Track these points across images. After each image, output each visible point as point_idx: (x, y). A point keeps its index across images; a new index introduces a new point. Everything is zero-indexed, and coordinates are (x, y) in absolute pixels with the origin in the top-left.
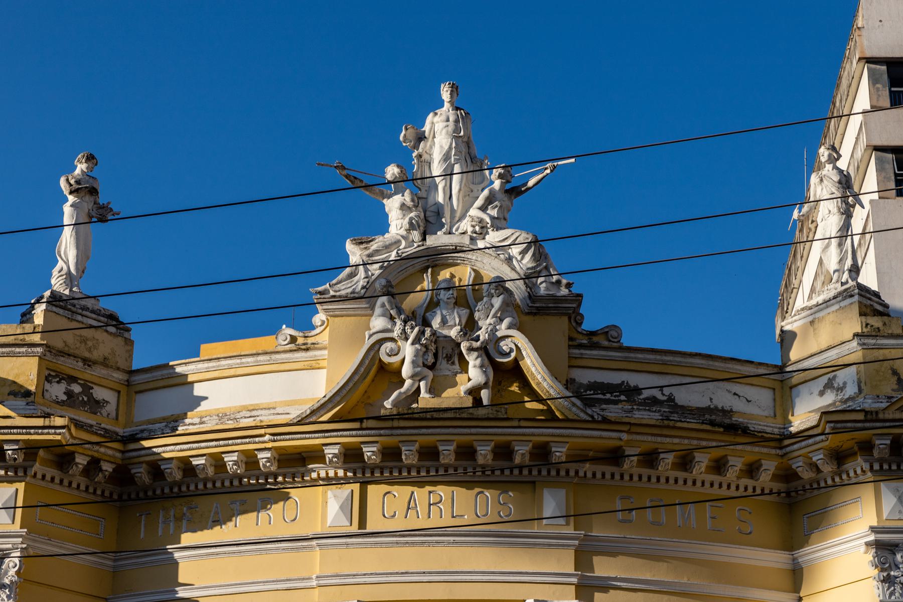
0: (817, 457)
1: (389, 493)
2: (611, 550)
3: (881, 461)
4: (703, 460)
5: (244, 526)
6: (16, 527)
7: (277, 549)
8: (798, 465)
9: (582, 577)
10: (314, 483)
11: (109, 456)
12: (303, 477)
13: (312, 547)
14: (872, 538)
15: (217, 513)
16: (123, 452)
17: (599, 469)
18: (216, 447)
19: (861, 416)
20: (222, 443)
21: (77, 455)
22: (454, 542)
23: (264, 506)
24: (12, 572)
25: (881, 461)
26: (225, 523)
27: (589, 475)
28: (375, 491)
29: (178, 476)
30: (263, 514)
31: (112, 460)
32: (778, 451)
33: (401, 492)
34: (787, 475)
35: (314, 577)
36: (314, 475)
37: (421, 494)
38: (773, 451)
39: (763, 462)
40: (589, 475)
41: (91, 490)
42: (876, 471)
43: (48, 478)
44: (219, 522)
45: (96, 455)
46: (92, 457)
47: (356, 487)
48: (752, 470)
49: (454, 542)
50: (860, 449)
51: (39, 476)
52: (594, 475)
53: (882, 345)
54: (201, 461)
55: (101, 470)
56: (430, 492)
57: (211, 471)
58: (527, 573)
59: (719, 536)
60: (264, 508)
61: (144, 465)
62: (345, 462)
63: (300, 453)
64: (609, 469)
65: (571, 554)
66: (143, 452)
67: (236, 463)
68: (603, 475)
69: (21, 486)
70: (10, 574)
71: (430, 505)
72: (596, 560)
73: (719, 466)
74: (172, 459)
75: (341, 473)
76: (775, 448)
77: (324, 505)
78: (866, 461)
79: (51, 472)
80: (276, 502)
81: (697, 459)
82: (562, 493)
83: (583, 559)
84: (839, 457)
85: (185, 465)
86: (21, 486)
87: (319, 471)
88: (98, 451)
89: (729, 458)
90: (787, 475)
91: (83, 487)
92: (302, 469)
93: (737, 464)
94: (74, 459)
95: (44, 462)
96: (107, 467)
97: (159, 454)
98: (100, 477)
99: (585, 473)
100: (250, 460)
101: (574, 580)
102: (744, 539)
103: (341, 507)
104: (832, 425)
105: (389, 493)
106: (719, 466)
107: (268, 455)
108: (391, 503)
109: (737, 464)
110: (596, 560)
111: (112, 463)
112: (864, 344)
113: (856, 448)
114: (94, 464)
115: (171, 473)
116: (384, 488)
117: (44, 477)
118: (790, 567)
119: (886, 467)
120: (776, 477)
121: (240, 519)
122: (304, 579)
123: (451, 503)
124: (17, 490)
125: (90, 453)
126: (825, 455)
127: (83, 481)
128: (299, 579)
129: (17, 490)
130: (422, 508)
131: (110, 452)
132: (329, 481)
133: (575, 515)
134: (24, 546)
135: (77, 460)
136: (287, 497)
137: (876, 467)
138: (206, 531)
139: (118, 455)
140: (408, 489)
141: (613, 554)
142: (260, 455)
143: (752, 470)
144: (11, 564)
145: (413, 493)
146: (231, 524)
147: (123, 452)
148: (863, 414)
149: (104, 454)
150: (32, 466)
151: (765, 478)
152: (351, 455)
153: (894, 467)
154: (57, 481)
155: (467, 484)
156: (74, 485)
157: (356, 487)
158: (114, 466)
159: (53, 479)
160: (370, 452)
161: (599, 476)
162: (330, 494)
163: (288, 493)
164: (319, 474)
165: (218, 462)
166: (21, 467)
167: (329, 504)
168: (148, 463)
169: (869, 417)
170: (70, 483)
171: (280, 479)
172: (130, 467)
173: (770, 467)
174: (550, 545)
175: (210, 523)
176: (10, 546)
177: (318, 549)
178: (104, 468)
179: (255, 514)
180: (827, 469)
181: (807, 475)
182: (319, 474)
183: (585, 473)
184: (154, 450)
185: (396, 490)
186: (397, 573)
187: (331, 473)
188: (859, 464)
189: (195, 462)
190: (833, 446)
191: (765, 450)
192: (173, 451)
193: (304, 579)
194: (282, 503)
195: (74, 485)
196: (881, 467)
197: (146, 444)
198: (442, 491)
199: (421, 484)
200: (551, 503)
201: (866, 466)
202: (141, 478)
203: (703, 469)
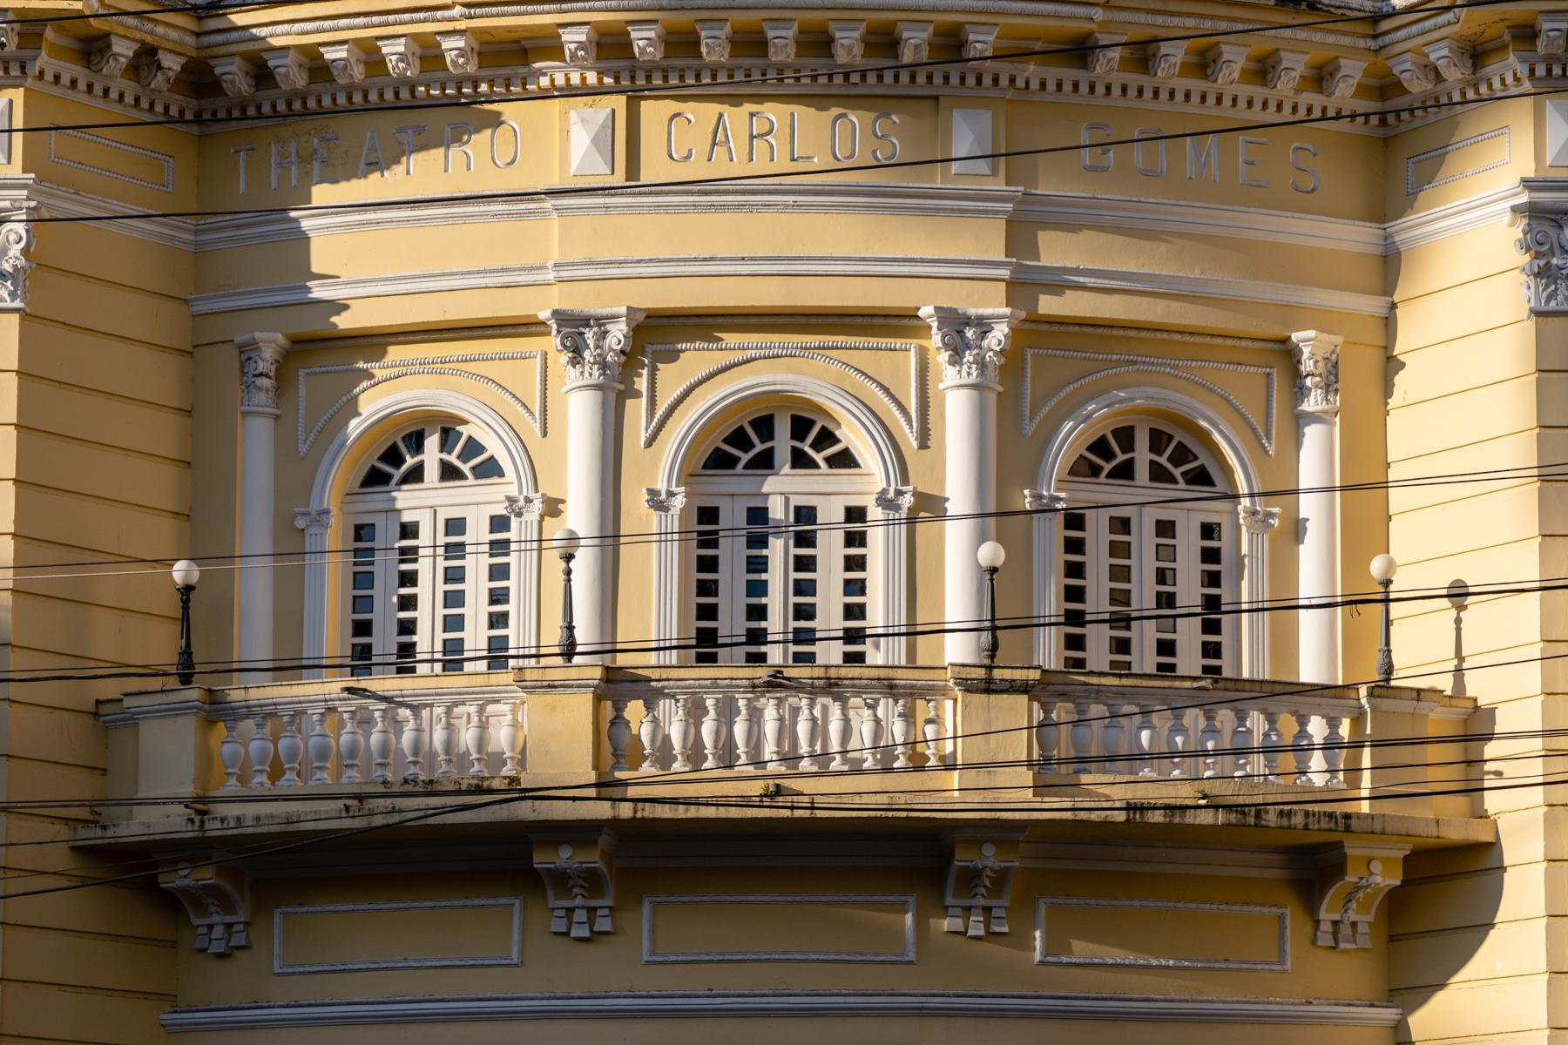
0: (1438, 54)
1: (678, 115)
2: (1069, 220)
3: (1549, 61)
4: (1236, 58)
5: (423, 172)
6: (15, 170)
7: (483, 215)
8: (1404, 69)
9: (1018, 268)
10: (545, 96)
11: (174, 41)
12: (524, 85)
13: (544, 212)
14: (1524, 198)
15: (373, 149)
16: (198, 35)
17: (1053, 73)
18: (365, 27)
20: (375, 19)
21: (114, 40)
22: (796, 205)
23: (456, 136)
24: (15, 250)
25: (1549, 61)
26: (388, 168)
27: (1035, 85)
28: (653, 112)
29: (300, 80)
30: (455, 152)
31: (179, 49)
33: (702, 114)
34: (1385, 87)
35: (550, 264)
36: (545, 82)
37: (736, 117)
40: (1035, 85)
41: (145, 104)
42: (1540, 79)
43: (65, 80)
44: (377, 164)
45: (149, 39)
46: (143, 43)
47: (620, 102)
48: (1321, 77)
49: (796, 205)
50: (1515, 37)
51: (49, 77)
52: (1043, 85)
54: (339, 53)
55: (160, 67)
56: (752, 115)
57: (358, 72)
58: (922, 261)
59: (1258, 196)
60: (457, 139)
61: (237, 59)
62: (599, 58)
63: (517, 41)
64: (1069, 74)
65: (998, 228)
66: (234, 35)
67: (403, 57)
68: (1059, 85)
69: (18, 95)
70: (11, 253)
71: (752, 137)
72: (1043, 237)
73: (1264, 70)
74: (285, 48)
75: (592, 78)
76: (1364, 36)
77: (562, 135)
78: (1522, 60)
79: (69, 70)
80: (478, 131)
81: (1225, 57)
82: (986, 117)
83: (1020, 236)
84: (1477, 54)
85: (315, 64)
86: (18, 95)
87: (552, 73)
88: (151, 33)
89: (1283, 54)
90: (1385, 87)
91: (129, 99)
92: (522, 70)
93: (1295, 65)
94: (109, 46)
95: (56, 52)
96: (172, 63)
97: (263, 39)
98: (159, 81)
99: (1027, 83)
100: (428, 53)
101: (1005, 273)
102: (1303, 200)
103: (595, 141)
105: (678, 115)
106: (1264, 70)
107: (460, 43)
108: (681, 132)
109: (1295, 65)
110: (1043, 237)
111: (179, 54)
113: (1507, 37)
114: (147, 56)
115: (287, 76)
116: (673, 106)
117: (57, 78)
118: (1378, 251)
120: (1362, 91)
121: (416, 160)
122: (532, 268)
123: (790, 133)
124: (11, 102)
125: (138, 35)
126: (1451, 50)
127: (131, 89)
128: (524, 269)
129: (11, 102)
130: (738, 144)
131: (174, 34)
132: (569, 92)
133: (1009, 156)
134: (33, 204)
135: (116, 49)
136: (496, 121)
137: (1541, 71)
138: (355, 182)
139: (190, 40)
140: (713, 109)
141: (1073, 227)
142: (447, 44)
143: (1321, 77)
144: (12, 237)
145: (721, 115)
146: (399, 169)
147: (198, 35)
149: (165, 38)
150: (34, 59)
151: (1344, 93)
152: (610, 46)
154: (82, 86)
155: (818, 100)
156: (114, 95)
157: (620, 102)
158: (183, 60)
159: (74, 83)
160: (643, 40)
161: (1051, 86)
162: (573, 116)
163: (499, 114)
164: (553, 81)
165: (370, 55)
166: (15, 59)
167: (572, 134)
168: (246, 56)
170: (106, 91)
171: (484, 88)
172: (212, 62)
173: (1353, 71)
174: (963, 211)
175: (362, 166)
176: (7, 204)
177: (555, 215)
178: (165, 64)
179: (442, 150)
180: (1454, 75)
181: (1418, 86)
182: (553, 81)
183: (1027, 83)
184: (254, 31)
185: (691, 109)
186: (695, 259)
187: (575, 79)
188: (1509, 67)
189: (330, 54)
190: (1468, 32)
191: (1346, 41)
192: (288, 34)
193: (532, 268)
194: (488, 132)
195: (114, 95)
196: (1549, 71)
197: (239, 19)
198: (774, 112)
199: (735, 100)
200: (967, 133)
201: (1522, 70)
202: (233, 82)
203: (1236, 75)
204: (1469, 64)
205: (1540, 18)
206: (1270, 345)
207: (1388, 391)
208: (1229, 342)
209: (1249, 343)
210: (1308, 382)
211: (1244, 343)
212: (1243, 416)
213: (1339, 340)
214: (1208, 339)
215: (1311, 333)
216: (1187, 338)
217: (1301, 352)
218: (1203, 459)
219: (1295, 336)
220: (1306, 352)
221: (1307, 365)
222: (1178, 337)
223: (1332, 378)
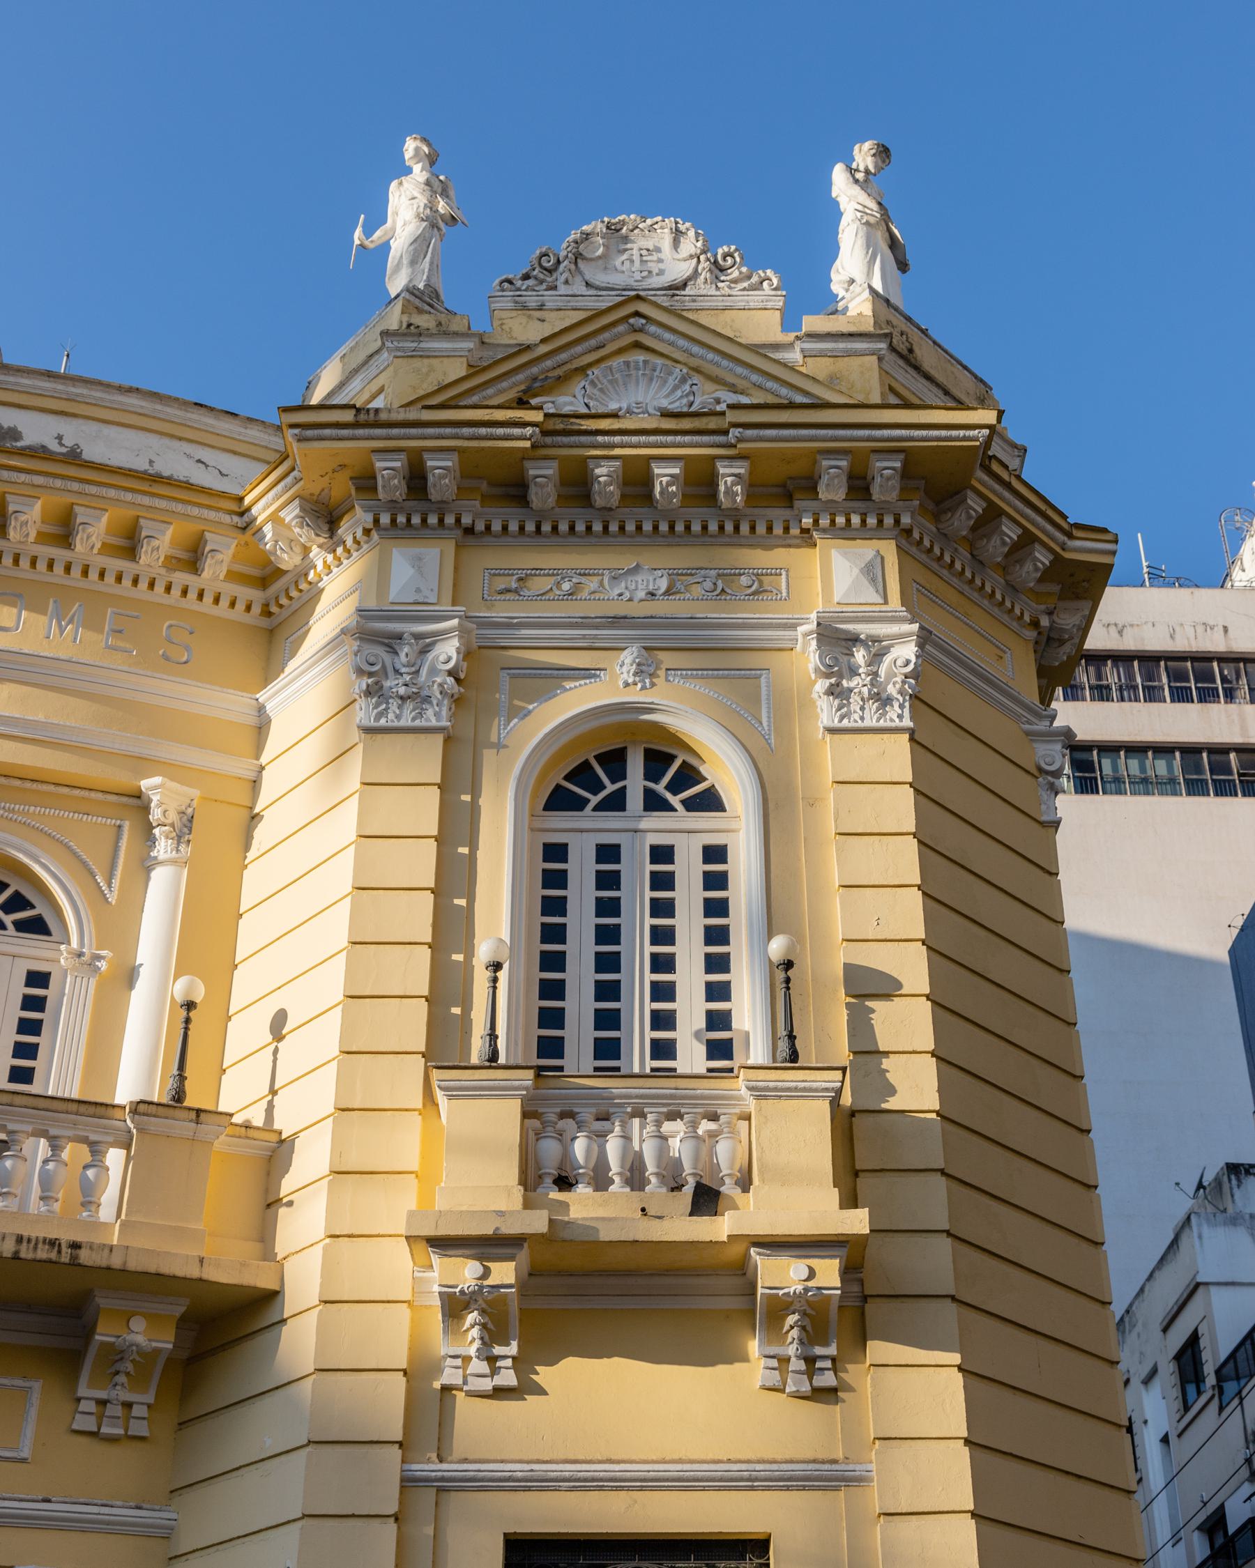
19: (348, 416)
32: (236, 519)
38: (226, 519)
39: (208, 535)
42: (386, 529)
50: (359, 489)
53: (428, 349)
78: (367, 509)
104: (296, 431)
112: (398, 349)
119: (401, 519)
126: (302, 509)
137: (385, 519)
148: (353, 412)
153: (416, 520)
169: (362, 417)
191: (212, 515)
204: (326, 527)
205: (374, 457)
206: (124, 799)
207: (247, 847)
208: (77, 792)
209: (100, 796)
210: (156, 831)
211: (93, 795)
212: (84, 863)
213: (195, 793)
214: (52, 788)
215: (157, 780)
216: (28, 785)
217: (150, 801)
218: (40, 909)
219: (145, 784)
220: (155, 799)
221: (156, 814)
222: (17, 783)
223: (186, 830)
